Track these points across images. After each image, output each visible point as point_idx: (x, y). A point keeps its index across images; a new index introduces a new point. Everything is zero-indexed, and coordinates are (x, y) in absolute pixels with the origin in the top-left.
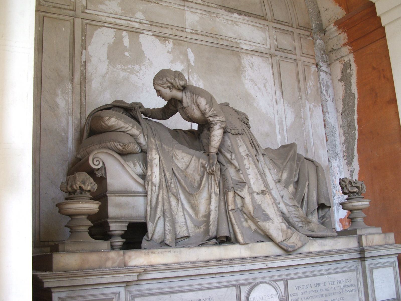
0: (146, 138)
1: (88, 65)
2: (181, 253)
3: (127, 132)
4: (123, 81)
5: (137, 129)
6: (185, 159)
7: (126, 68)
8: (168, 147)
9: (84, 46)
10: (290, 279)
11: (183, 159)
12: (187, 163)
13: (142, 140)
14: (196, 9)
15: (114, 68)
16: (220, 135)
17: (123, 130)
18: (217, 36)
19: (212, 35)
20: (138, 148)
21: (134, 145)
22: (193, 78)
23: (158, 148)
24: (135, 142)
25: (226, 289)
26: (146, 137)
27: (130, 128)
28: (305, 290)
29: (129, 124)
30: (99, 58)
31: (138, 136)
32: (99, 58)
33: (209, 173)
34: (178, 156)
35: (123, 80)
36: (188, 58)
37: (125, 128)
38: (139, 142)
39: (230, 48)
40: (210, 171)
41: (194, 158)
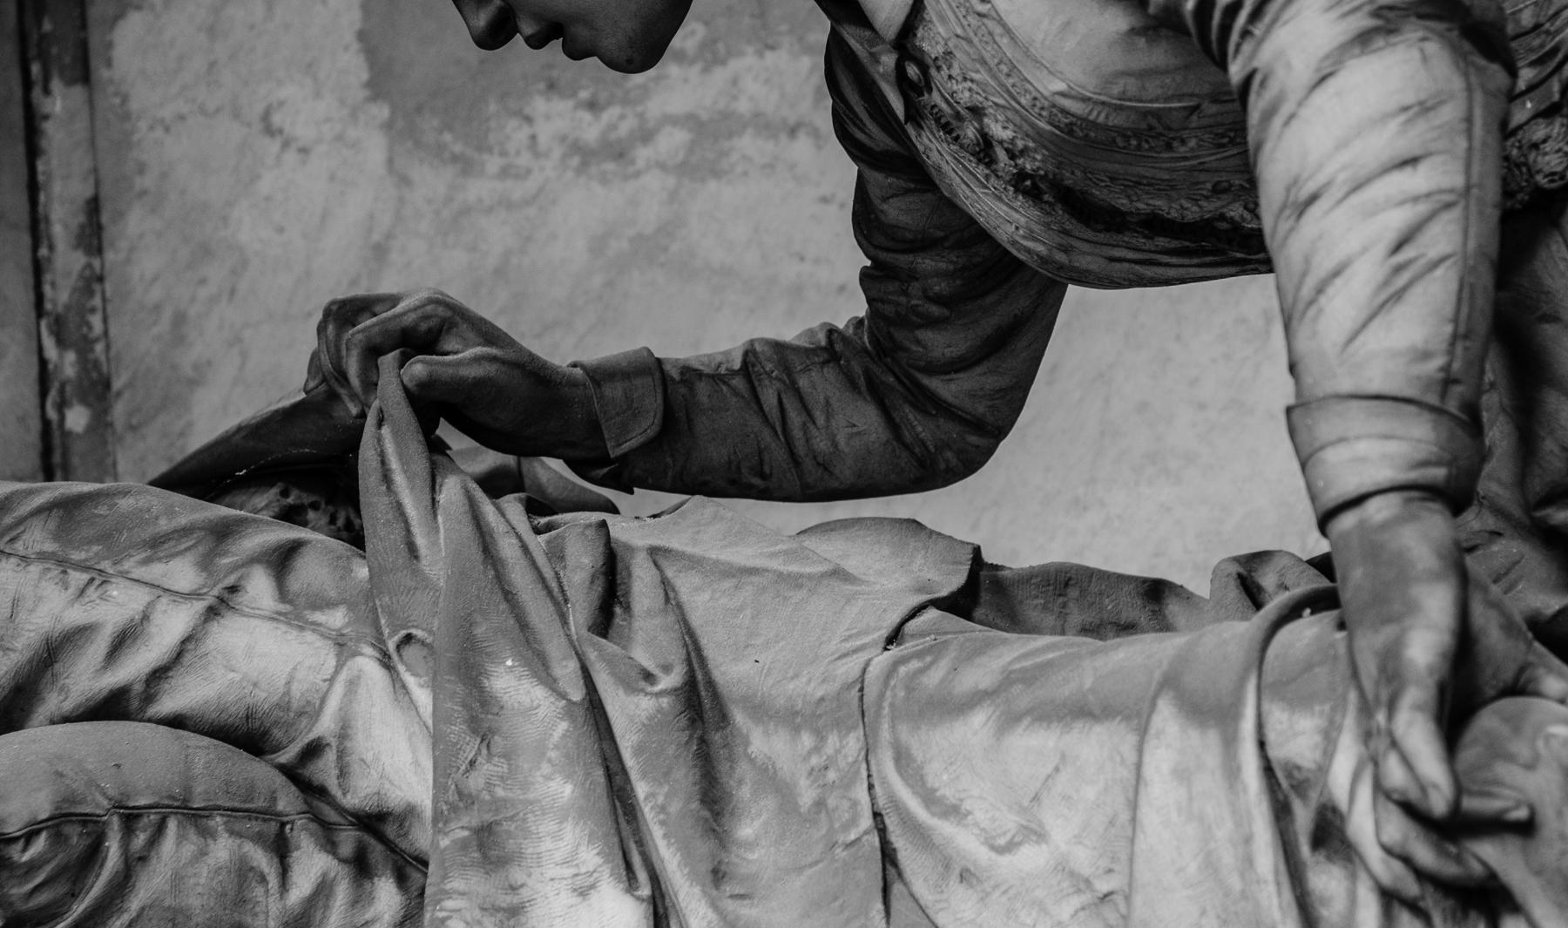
0: (423, 697)
1: (133, 227)
3: (168, 704)
4: (610, 284)
5: (295, 610)
6: (1061, 830)
7: (625, 128)
8: (807, 740)
11: (1035, 833)
12: (1103, 886)
13: (391, 752)
15: (467, 167)
16: (1407, 144)
17: (85, 678)
20: (360, 899)
21: (261, 859)
23: (641, 789)
24: (288, 800)
26: (410, 680)
27: (172, 624)
29: (155, 571)
30: (266, 117)
31: (323, 701)
32: (266, 117)
33: (1411, 888)
34: (953, 811)
35: (598, 280)
37: (98, 647)
38: (359, 794)
40: (1397, 828)
41: (1160, 759)
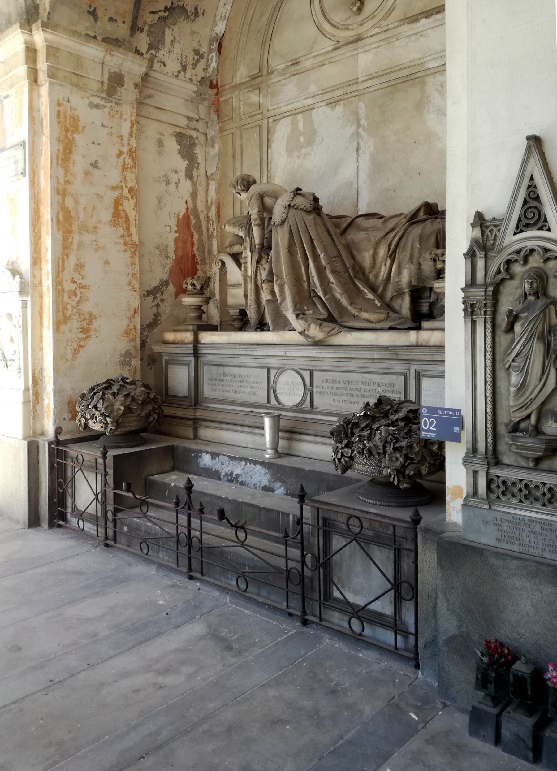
2: (230, 336)
9: (269, 146)
10: (315, 370)
14: (372, 44)
18: (396, 69)
19: (390, 70)
22: (362, 139)
25: (260, 369)
28: (333, 385)
36: (358, 116)
39: (413, 77)
